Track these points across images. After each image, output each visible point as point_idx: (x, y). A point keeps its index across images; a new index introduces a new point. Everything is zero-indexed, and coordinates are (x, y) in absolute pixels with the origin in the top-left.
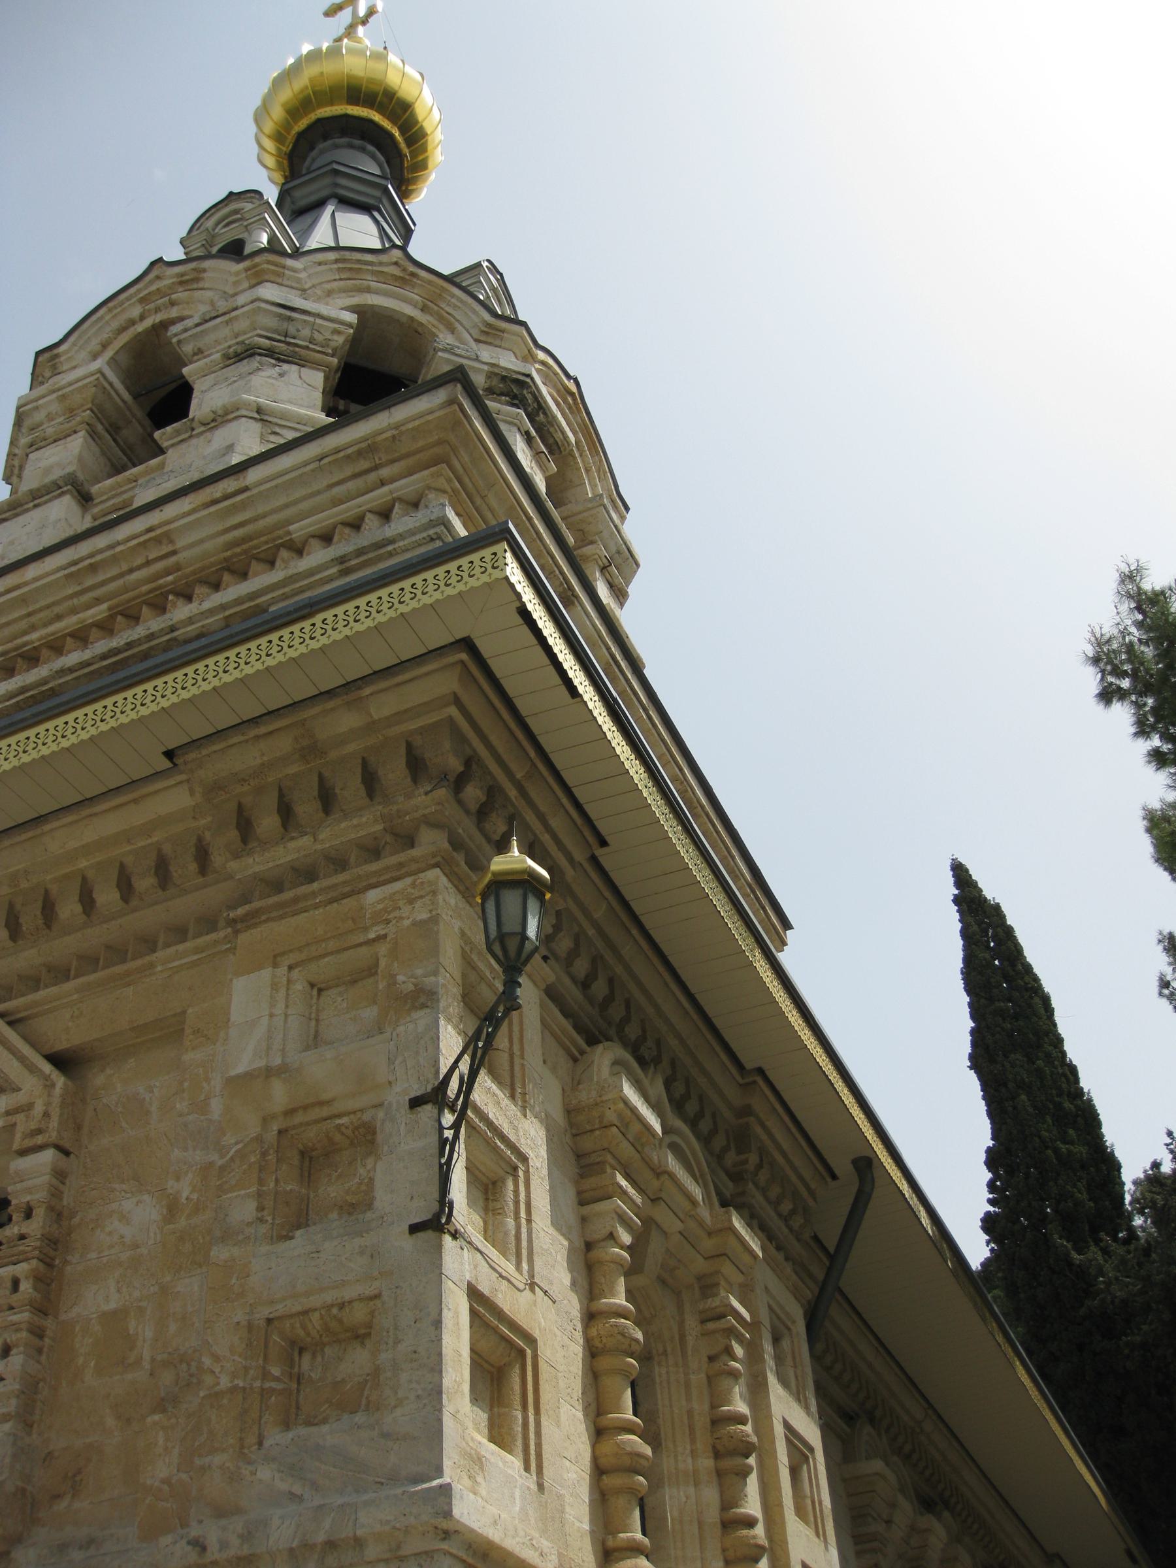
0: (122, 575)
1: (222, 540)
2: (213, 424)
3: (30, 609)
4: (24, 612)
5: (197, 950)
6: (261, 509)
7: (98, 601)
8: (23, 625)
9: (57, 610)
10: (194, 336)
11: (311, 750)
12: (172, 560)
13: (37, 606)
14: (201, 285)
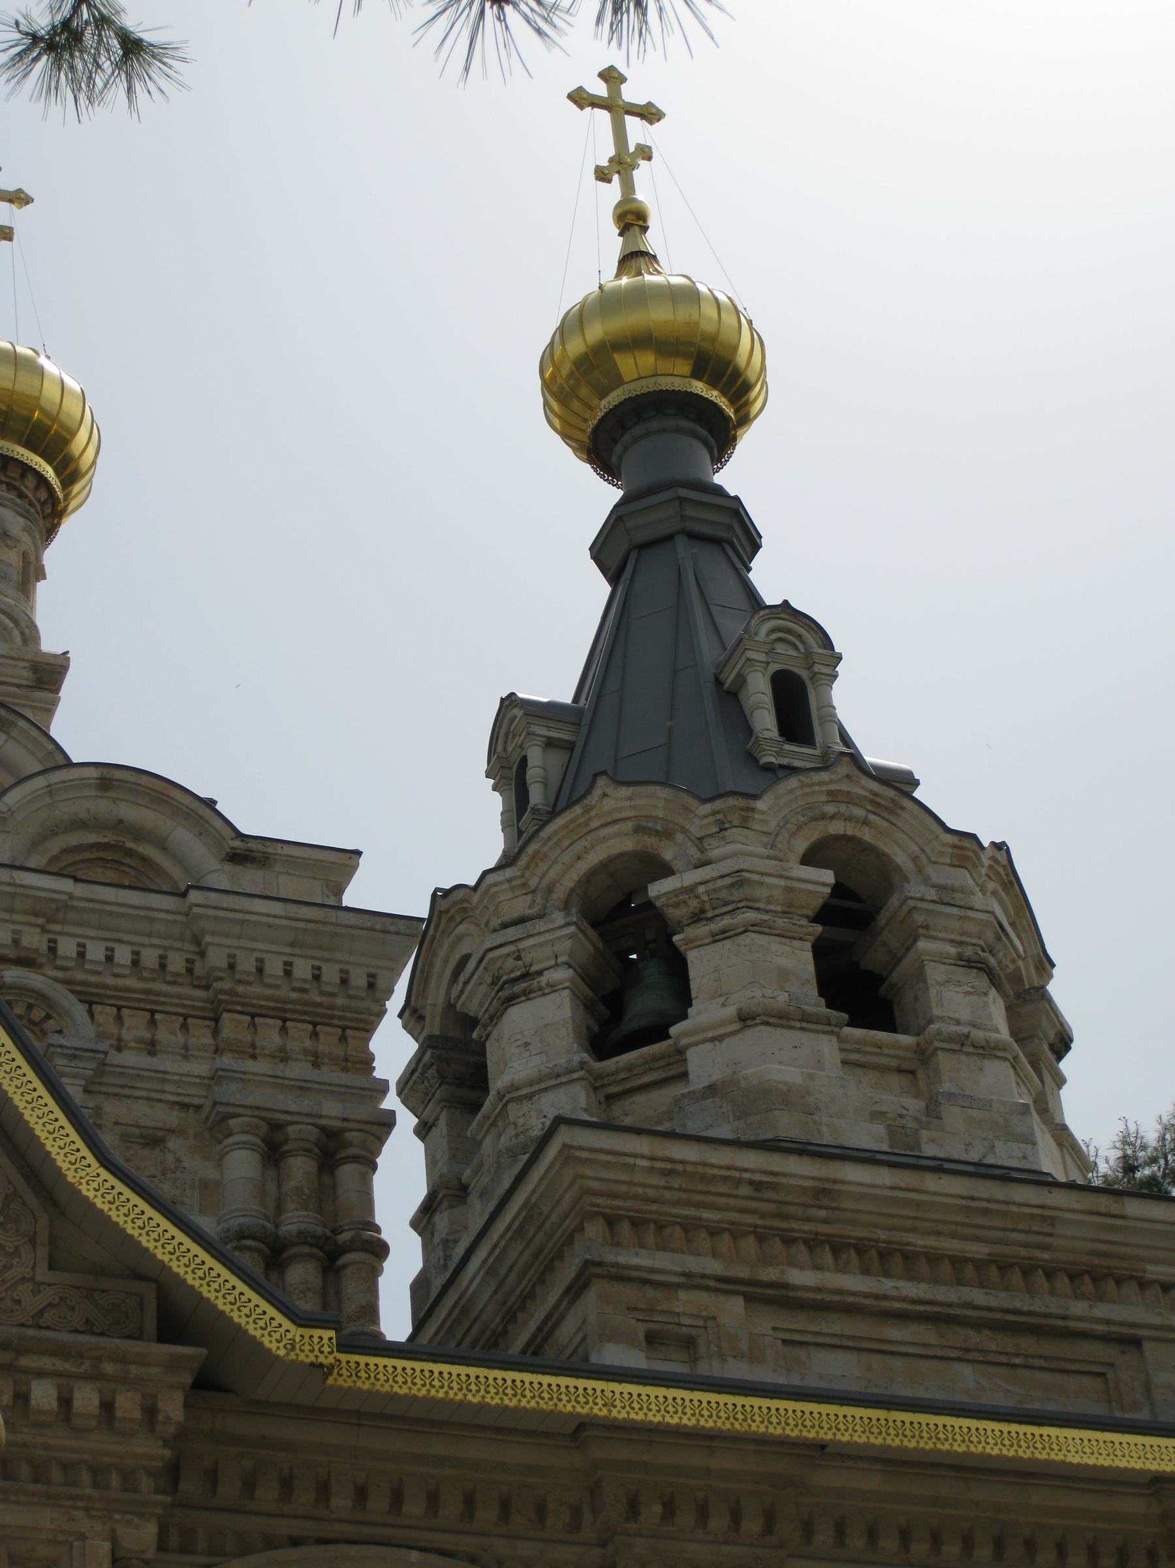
0: (1004, 1229)
2: (981, 1051)
3: (920, 1215)
4: (913, 1214)
7: (977, 1239)
8: (908, 1223)
10: (929, 911)
12: (1048, 1240)
14: (893, 819)
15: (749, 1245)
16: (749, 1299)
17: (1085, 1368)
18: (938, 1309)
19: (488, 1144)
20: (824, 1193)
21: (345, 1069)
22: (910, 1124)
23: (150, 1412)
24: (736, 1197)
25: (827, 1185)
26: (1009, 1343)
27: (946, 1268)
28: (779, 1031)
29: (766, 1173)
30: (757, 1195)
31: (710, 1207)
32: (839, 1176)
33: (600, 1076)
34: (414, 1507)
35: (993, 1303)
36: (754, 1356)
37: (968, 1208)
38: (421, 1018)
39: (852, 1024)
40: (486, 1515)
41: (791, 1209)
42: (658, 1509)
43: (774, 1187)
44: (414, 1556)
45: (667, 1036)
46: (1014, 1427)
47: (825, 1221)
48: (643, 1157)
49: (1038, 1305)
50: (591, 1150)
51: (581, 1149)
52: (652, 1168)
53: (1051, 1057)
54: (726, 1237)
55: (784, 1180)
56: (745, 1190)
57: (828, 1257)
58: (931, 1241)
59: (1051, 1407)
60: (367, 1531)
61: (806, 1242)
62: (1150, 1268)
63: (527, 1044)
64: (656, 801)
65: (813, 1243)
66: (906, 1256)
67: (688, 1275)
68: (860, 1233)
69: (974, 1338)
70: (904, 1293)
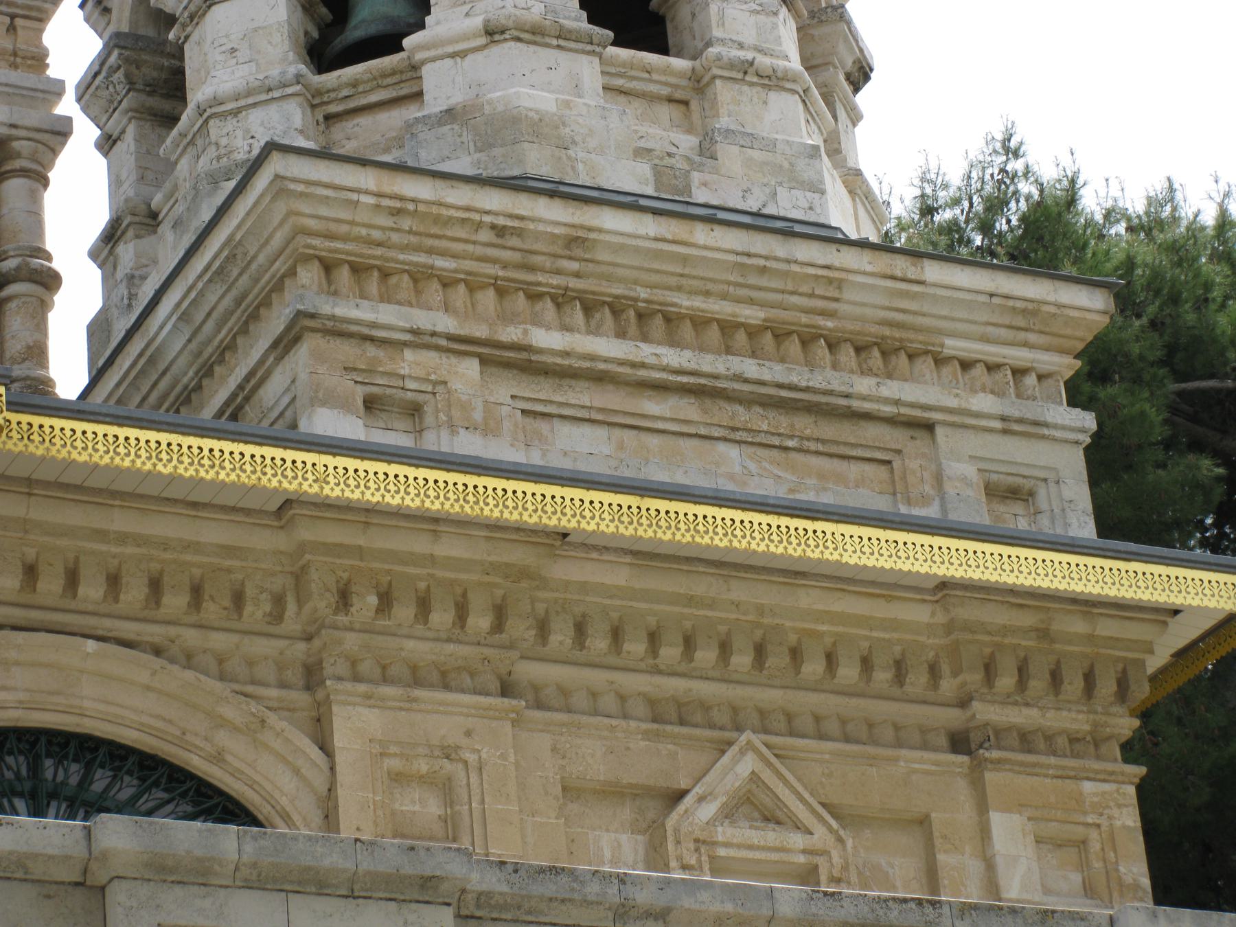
1: (883, 314)
2: (766, 82)
3: (686, 271)
4: (679, 270)
5: (937, 764)
6: (926, 308)
7: (751, 302)
8: (673, 281)
9: (710, 286)
11: (1044, 634)
12: (834, 305)
13: (694, 273)
15: (488, 298)
16: (484, 361)
17: (868, 454)
18: (703, 381)
19: (184, 165)
20: (576, 242)
21: (14, 66)
22: (680, 164)
24: (474, 243)
25: (580, 233)
26: (783, 422)
27: (714, 333)
28: (532, 48)
29: (511, 216)
30: (499, 241)
31: (443, 253)
32: (595, 223)
33: (318, 93)
35: (767, 377)
36: (489, 428)
37: (742, 265)
38: (107, 10)
39: (616, 43)
40: (175, 602)
41: (538, 260)
42: (373, 600)
43: (519, 233)
44: (91, 645)
45: (400, 49)
46: (784, 521)
47: (577, 275)
48: (367, 192)
49: (818, 381)
50: (309, 183)
51: (294, 180)
52: (378, 206)
53: (848, 89)
54: (462, 288)
55: (531, 226)
56: (485, 236)
57: (578, 316)
58: (698, 303)
59: (827, 499)
60: (36, 616)
61: (554, 298)
62: (949, 342)
63: (233, 50)
65: (561, 300)
66: (668, 319)
67: (415, 332)
68: (618, 290)
69: (742, 415)
70: (665, 361)
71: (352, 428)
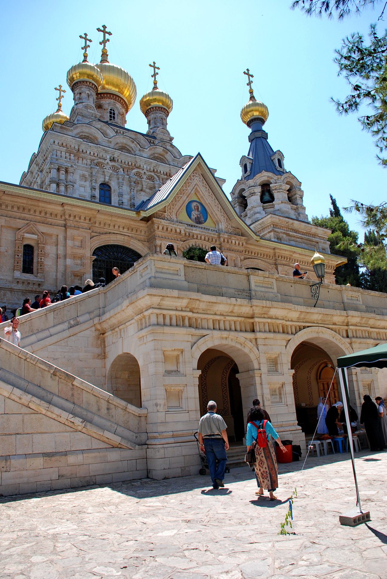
23: (243, 244)
34: (259, 255)
36: (286, 241)
40: (265, 256)
64: (270, 174)
71: (276, 240)
